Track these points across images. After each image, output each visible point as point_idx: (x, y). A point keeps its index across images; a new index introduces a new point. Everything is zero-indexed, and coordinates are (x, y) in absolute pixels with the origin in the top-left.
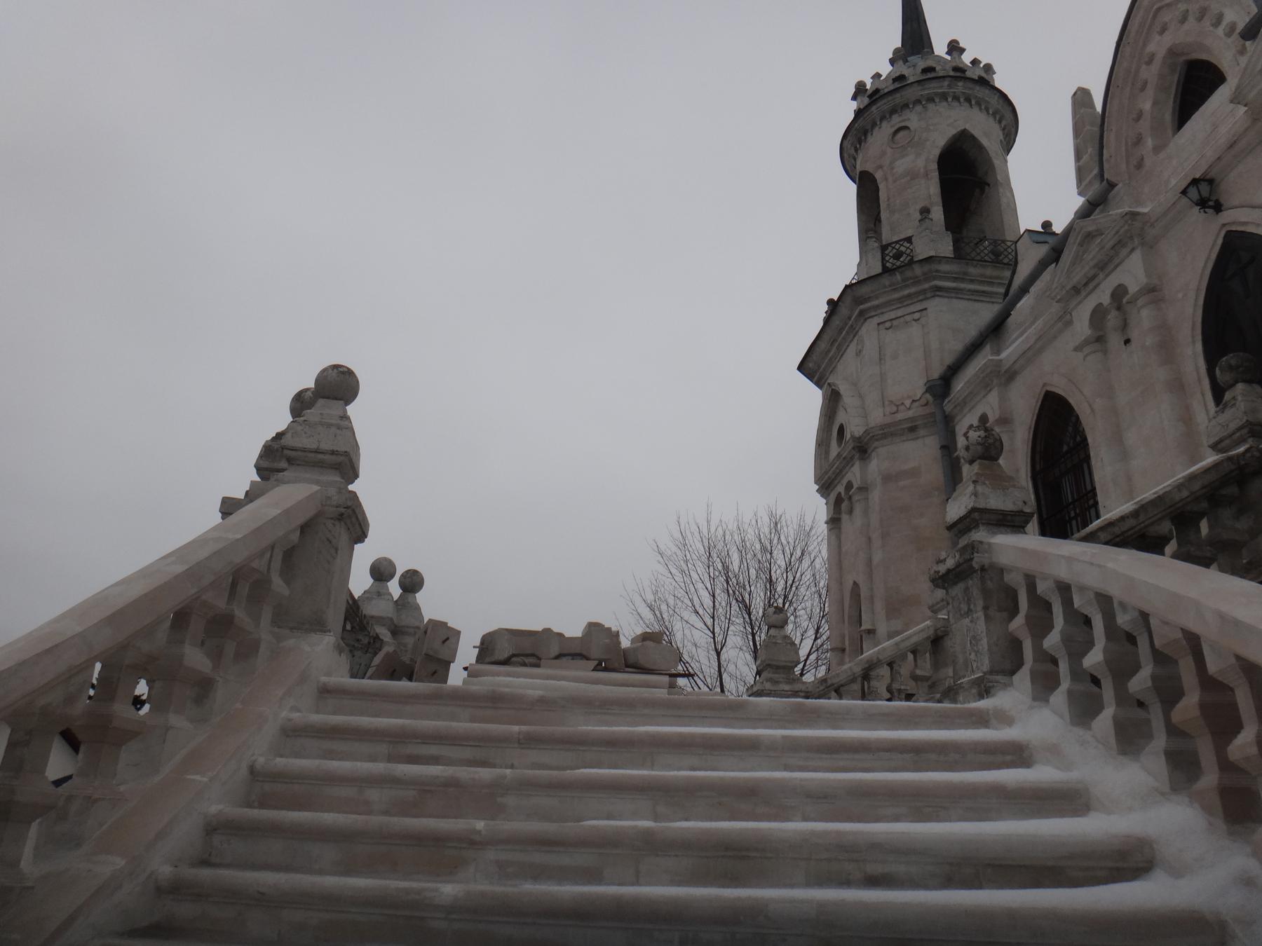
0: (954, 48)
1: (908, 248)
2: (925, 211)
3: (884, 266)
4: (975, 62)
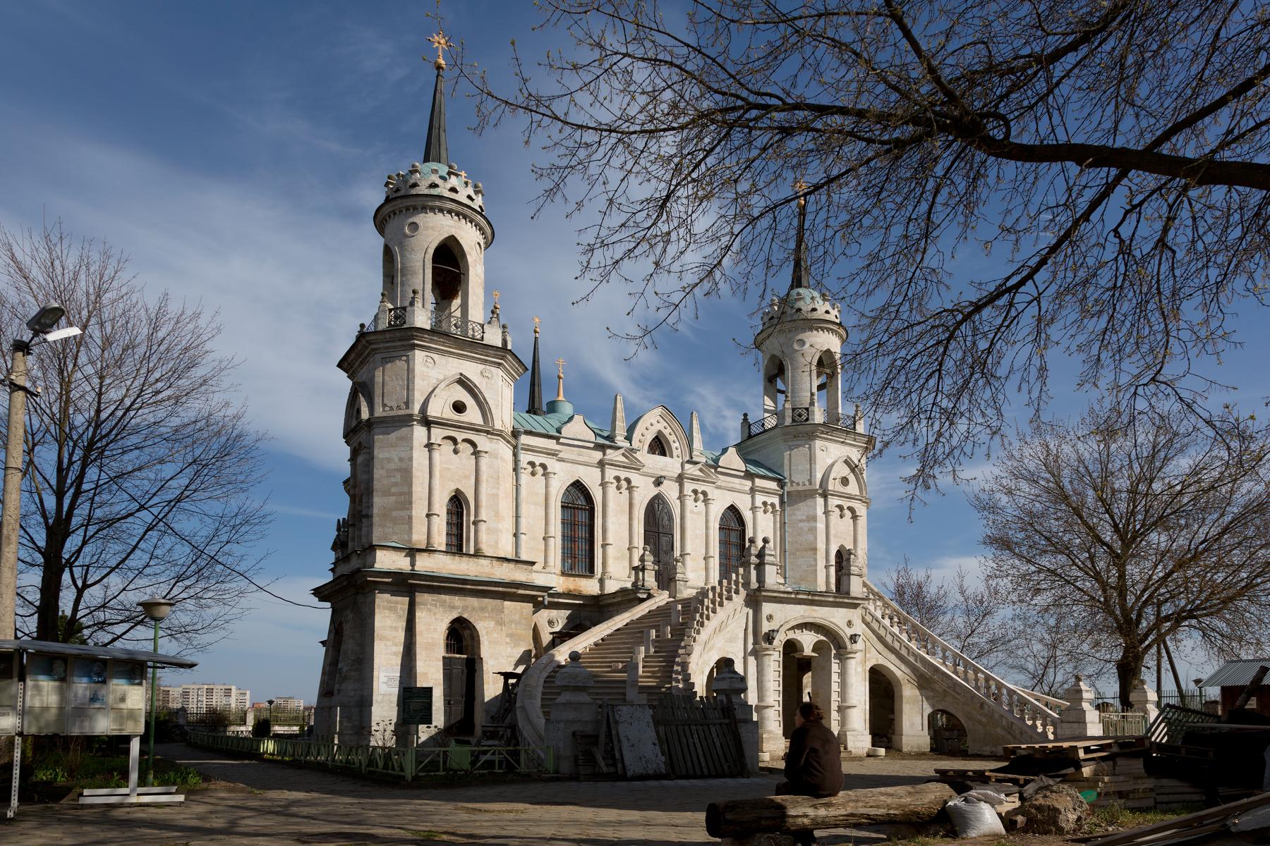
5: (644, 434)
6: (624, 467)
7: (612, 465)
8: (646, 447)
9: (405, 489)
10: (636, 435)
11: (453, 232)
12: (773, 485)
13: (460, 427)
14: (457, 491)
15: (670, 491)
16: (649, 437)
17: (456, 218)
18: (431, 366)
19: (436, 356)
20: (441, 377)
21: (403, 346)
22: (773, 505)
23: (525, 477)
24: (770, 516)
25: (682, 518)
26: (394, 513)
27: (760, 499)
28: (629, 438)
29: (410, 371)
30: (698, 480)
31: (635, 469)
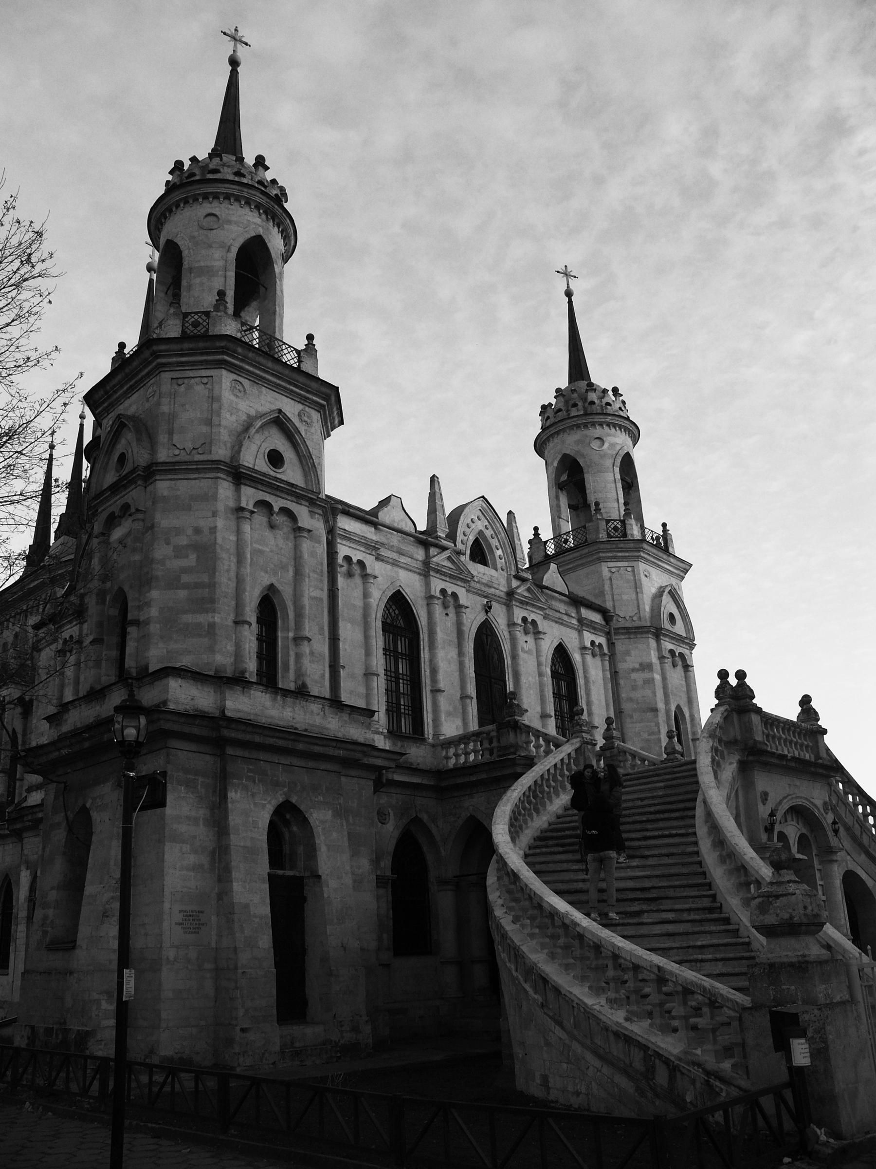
0: (260, 161)
1: (205, 321)
2: (221, 294)
3: (183, 331)
4: (274, 182)
5: (465, 538)
6: (451, 576)
7: (437, 571)
8: (468, 552)
9: (205, 578)
10: (460, 536)
11: (261, 231)
12: (596, 617)
13: (278, 488)
14: (272, 586)
15: (499, 618)
16: (472, 538)
17: (264, 216)
18: (239, 394)
19: (246, 383)
20: (253, 413)
21: (206, 362)
22: (600, 645)
23: (341, 581)
24: (598, 660)
25: (514, 657)
26: (188, 618)
27: (588, 637)
28: (452, 536)
29: (214, 398)
30: (527, 603)
31: (462, 580)
